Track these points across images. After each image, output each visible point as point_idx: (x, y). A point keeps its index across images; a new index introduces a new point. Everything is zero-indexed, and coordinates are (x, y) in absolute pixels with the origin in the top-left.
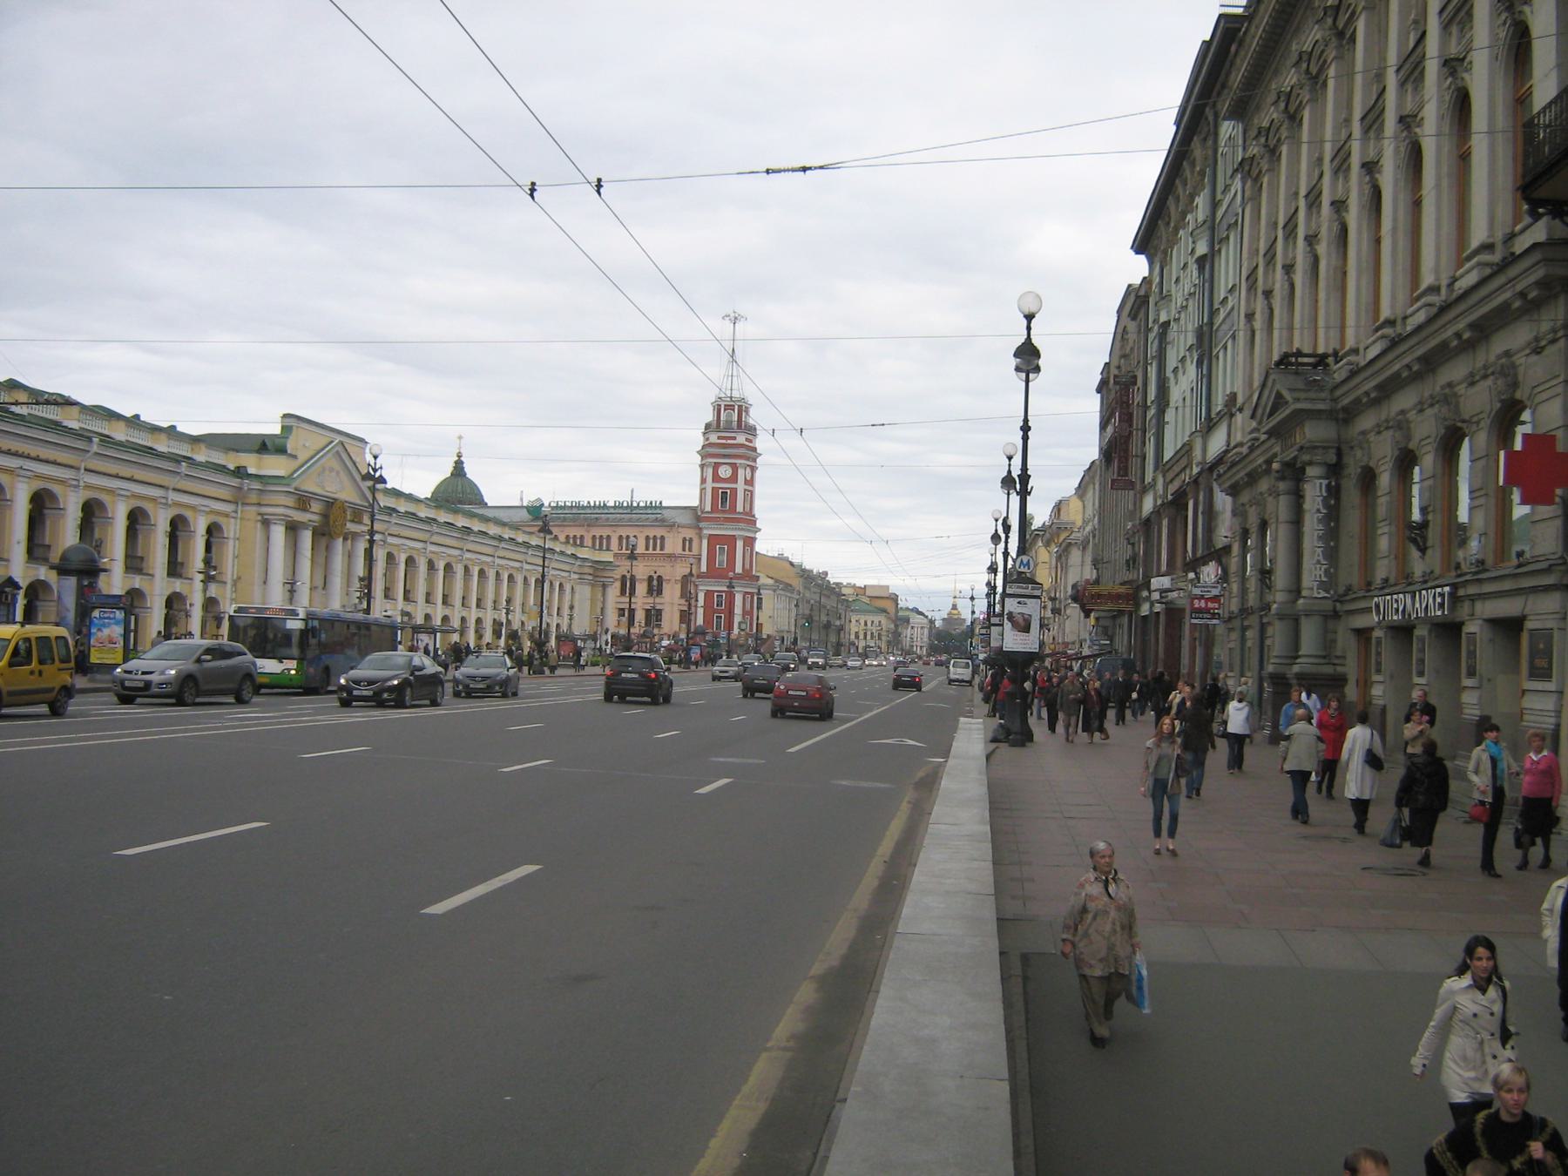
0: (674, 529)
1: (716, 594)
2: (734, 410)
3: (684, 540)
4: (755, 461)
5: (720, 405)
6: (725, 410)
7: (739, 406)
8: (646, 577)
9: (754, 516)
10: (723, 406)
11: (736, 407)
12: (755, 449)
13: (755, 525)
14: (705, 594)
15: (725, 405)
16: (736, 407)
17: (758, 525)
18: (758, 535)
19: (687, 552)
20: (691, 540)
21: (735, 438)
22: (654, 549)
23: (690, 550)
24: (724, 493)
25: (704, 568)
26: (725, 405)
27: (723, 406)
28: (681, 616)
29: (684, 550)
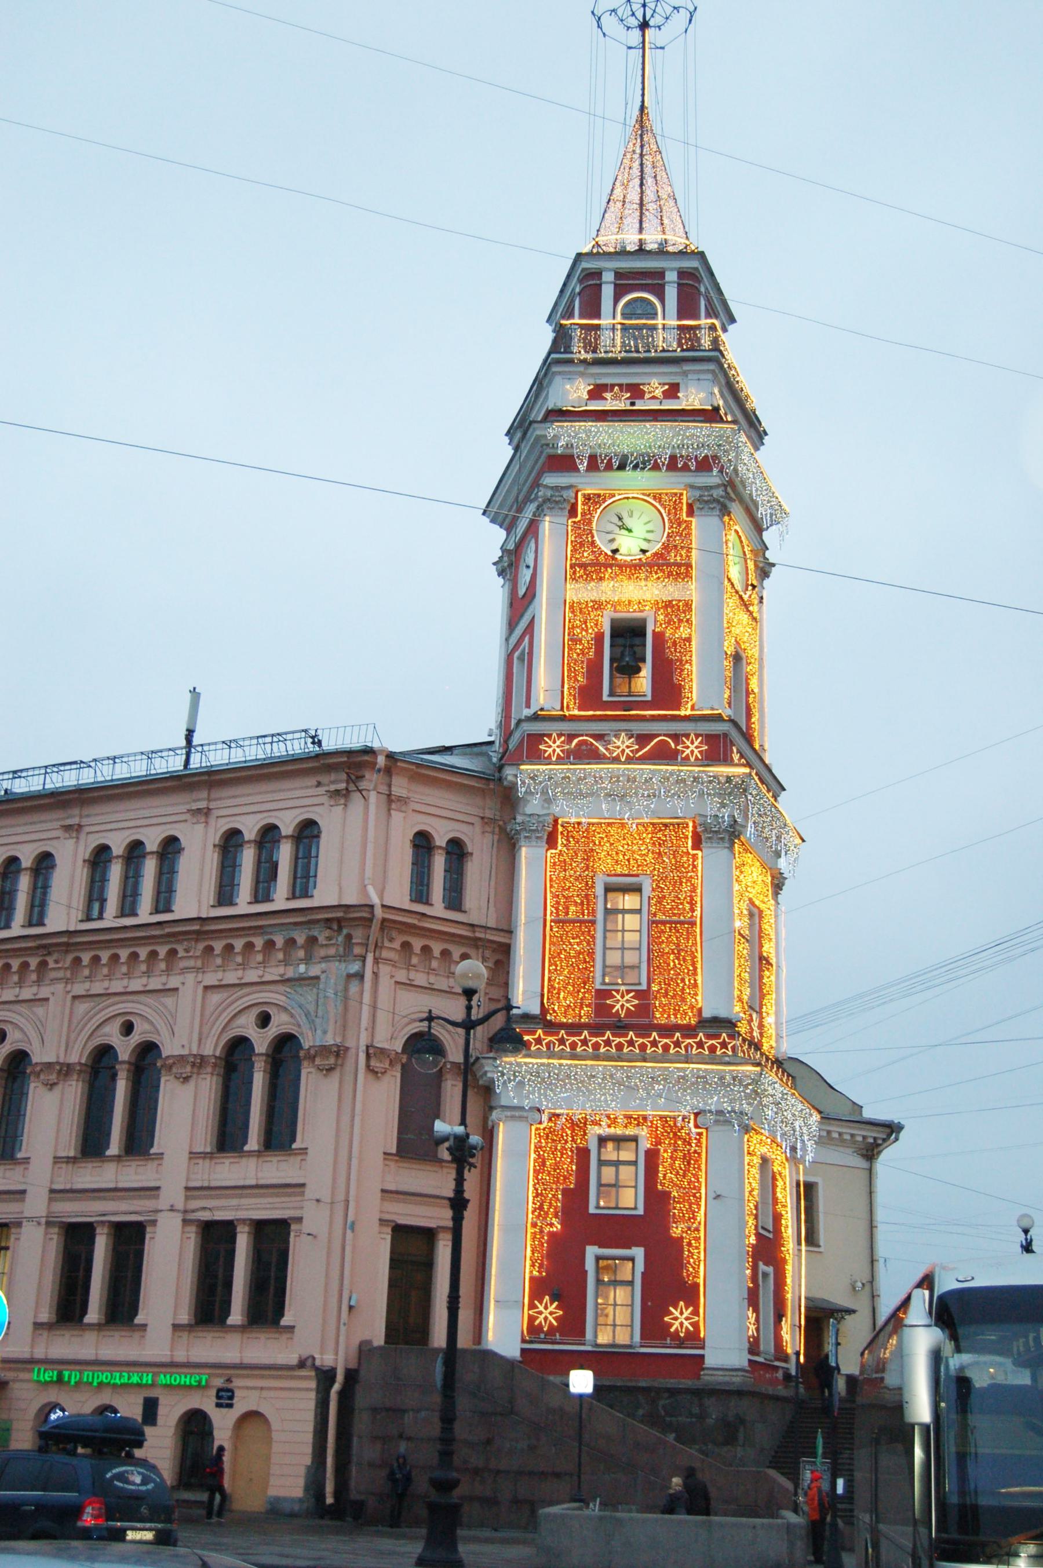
0: (371, 780)
2: (660, 292)
3: (422, 843)
5: (598, 274)
6: (619, 292)
7: (682, 274)
8: (213, 1047)
10: (608, 277)
11: (671, 276)
15: (618, 275)
16: (671, 276)
19: (437, 908)
20: (457, 850)
22: (262, 892)
23: (455, 899)
26: (618, 275)
27: (608, 277)
28: (395, 1263)
29: (420, 892)
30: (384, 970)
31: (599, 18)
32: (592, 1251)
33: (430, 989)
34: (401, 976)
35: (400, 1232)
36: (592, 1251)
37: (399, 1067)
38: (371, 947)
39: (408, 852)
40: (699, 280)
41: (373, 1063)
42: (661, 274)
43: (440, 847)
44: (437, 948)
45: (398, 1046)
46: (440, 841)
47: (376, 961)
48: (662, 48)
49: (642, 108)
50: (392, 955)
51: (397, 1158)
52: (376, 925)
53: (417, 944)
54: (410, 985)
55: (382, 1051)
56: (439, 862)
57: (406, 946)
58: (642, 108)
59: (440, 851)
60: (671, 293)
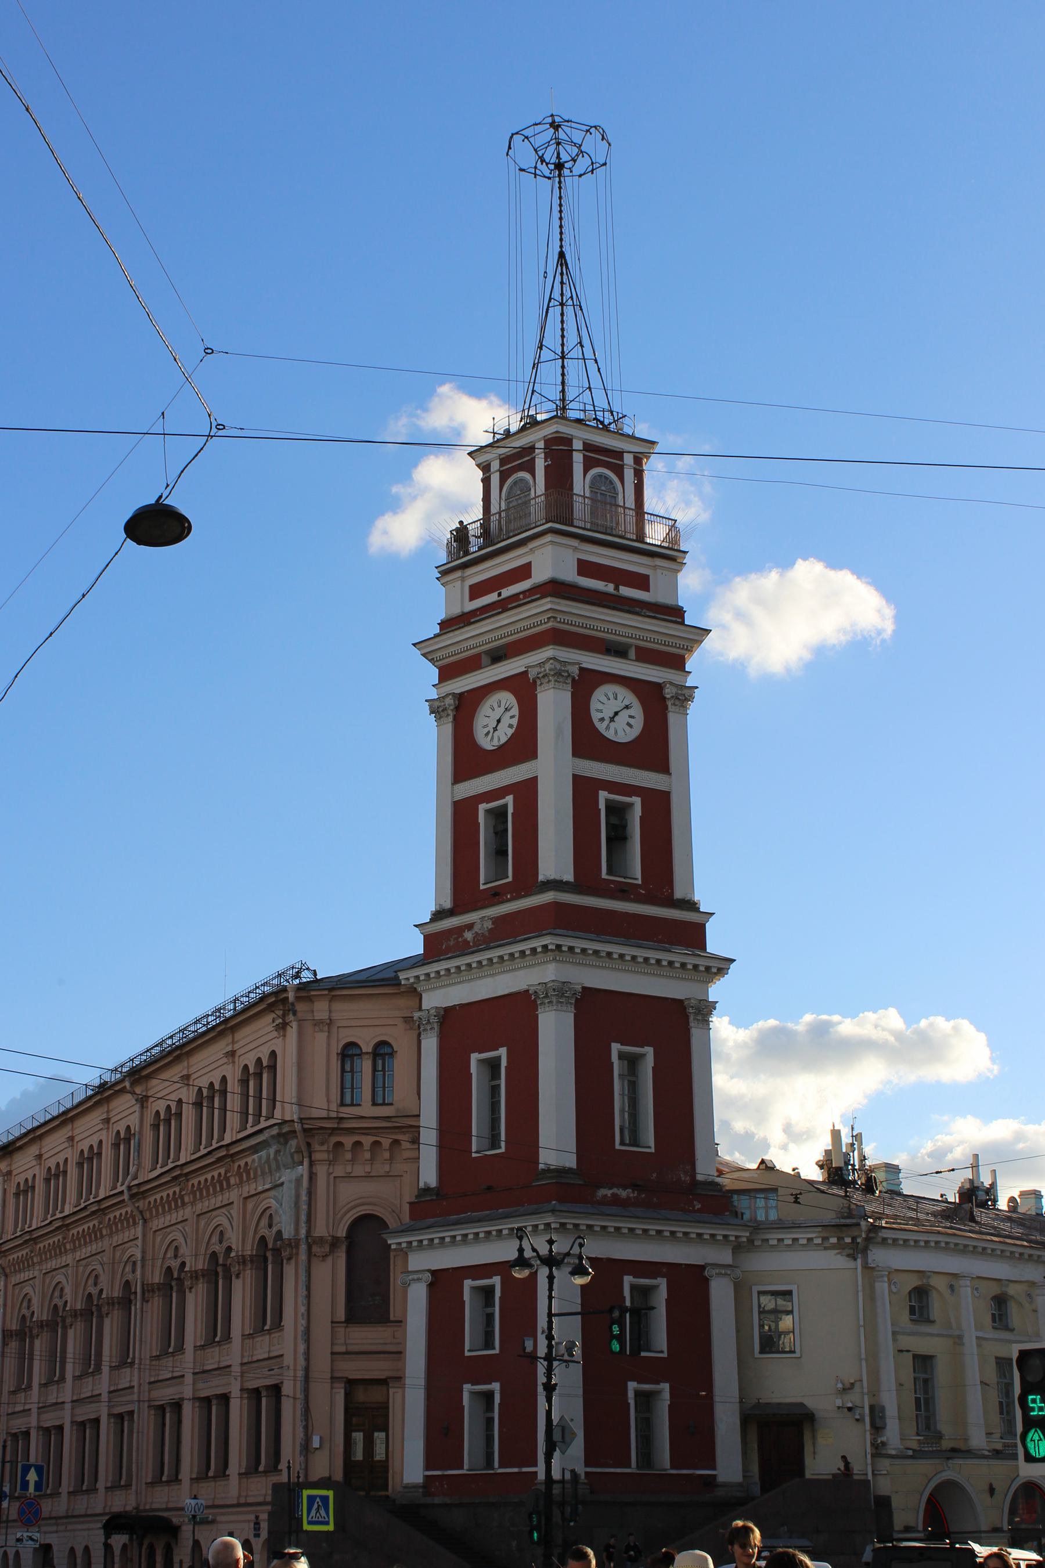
1: (468, 1283)
2: (531, 469)
3: (349, 1052)
4: (677, 663)
6: (504, 476)
9: (692, 906)
12: (675, 614)
13: (704, 947)
14: (431, 1286)
15: (503, 461)
17: (716, 943)
18: (716, 991)
20: (382, 1051)
21: (524, 572)
24: (499, 814)
25: (429, 1175)
26: (503, 461)
27: (495, 466)
30: (321, 1170)
31: (536, 168)
32: (467, 1387)
33: (368, 1177)
34: (339, 1170)
35: (351, 1384)
36: (467, 1387)
37: (344, 1248)
38: (305, 1154)
39: (335, 1064)
40: (568, 441)
41: (315, 1249)
42: (532, 448)
43: (367, 1053)
44: (367, 1141)
45: (342, 1232)
46: (367, 1047)
47: (312, 1163)
48: (605, 164)
49: (562, 255)
50: (325, 1156)
51: (345, 1325)
52: (300, 1135)
53: (348, 1141)
54: (349, 1177)
55: (321, 1238)
56: (367, 1065)
57: (339, 1144)
58: (562, 255)
59: (366, 1056)
60: (540, 464)
